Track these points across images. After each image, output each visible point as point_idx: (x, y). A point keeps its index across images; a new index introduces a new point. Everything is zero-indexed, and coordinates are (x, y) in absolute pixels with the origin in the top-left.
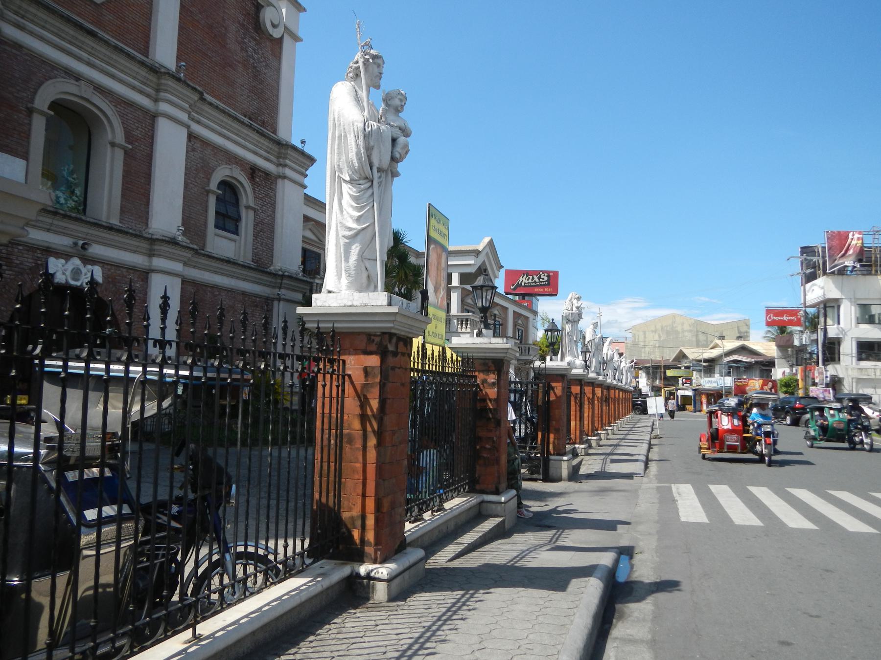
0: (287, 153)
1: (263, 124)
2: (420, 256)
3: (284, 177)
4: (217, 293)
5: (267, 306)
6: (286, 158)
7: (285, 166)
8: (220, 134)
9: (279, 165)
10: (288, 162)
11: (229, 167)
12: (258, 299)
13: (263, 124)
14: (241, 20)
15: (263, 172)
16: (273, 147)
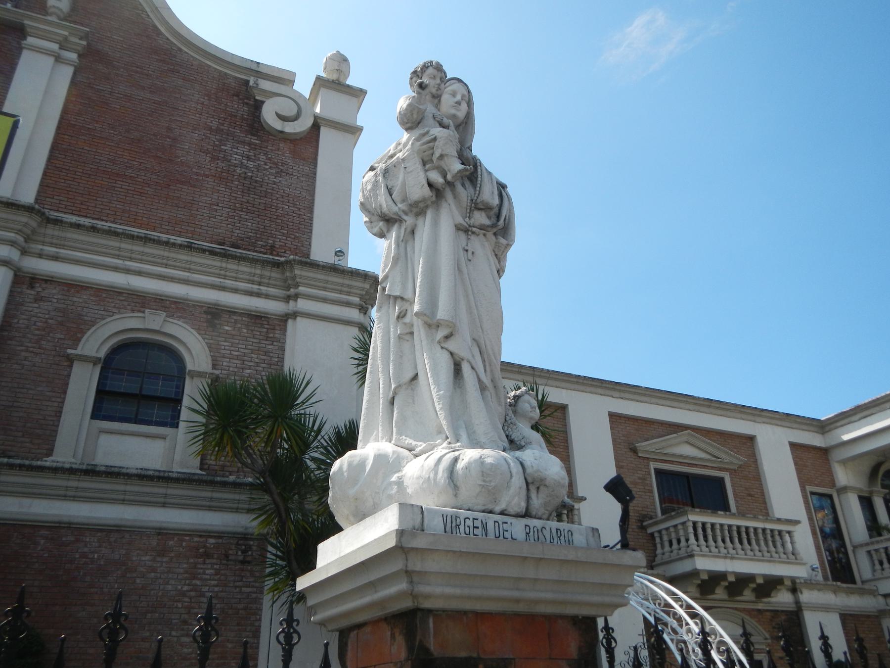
0: (294, 278)
1: (272, 249)
2: (827, 429)
3: (294, 315)
4: (72, 538)
5: (244, 552)
6: (297, 286)
7: (296, 297)
8: (116, 269)
9: (287, 299)
10: (302, 289)
11: (141, 315)
12: (212, 541)
13: (272, 249)
14: (214, 125)
15: (241, 314)
16: (274, 275)
